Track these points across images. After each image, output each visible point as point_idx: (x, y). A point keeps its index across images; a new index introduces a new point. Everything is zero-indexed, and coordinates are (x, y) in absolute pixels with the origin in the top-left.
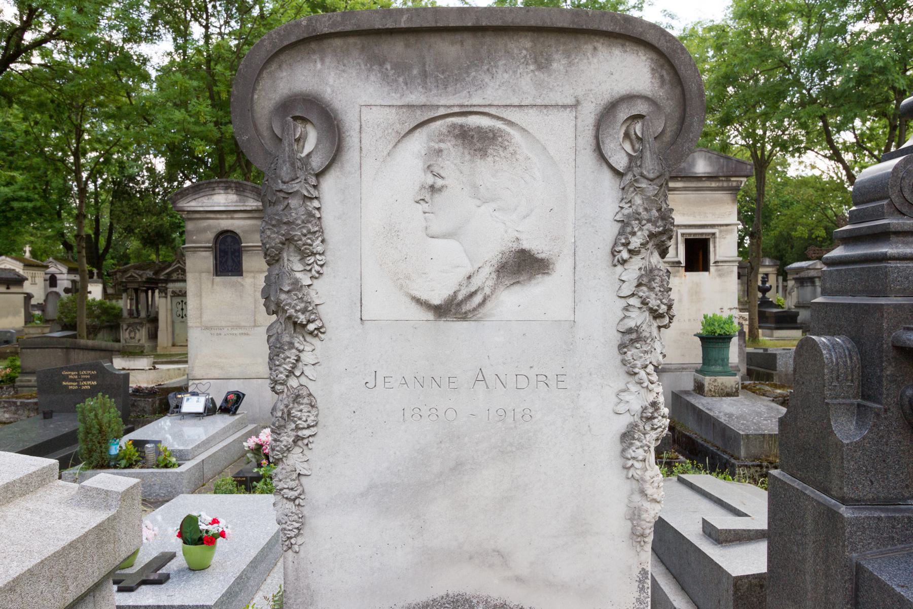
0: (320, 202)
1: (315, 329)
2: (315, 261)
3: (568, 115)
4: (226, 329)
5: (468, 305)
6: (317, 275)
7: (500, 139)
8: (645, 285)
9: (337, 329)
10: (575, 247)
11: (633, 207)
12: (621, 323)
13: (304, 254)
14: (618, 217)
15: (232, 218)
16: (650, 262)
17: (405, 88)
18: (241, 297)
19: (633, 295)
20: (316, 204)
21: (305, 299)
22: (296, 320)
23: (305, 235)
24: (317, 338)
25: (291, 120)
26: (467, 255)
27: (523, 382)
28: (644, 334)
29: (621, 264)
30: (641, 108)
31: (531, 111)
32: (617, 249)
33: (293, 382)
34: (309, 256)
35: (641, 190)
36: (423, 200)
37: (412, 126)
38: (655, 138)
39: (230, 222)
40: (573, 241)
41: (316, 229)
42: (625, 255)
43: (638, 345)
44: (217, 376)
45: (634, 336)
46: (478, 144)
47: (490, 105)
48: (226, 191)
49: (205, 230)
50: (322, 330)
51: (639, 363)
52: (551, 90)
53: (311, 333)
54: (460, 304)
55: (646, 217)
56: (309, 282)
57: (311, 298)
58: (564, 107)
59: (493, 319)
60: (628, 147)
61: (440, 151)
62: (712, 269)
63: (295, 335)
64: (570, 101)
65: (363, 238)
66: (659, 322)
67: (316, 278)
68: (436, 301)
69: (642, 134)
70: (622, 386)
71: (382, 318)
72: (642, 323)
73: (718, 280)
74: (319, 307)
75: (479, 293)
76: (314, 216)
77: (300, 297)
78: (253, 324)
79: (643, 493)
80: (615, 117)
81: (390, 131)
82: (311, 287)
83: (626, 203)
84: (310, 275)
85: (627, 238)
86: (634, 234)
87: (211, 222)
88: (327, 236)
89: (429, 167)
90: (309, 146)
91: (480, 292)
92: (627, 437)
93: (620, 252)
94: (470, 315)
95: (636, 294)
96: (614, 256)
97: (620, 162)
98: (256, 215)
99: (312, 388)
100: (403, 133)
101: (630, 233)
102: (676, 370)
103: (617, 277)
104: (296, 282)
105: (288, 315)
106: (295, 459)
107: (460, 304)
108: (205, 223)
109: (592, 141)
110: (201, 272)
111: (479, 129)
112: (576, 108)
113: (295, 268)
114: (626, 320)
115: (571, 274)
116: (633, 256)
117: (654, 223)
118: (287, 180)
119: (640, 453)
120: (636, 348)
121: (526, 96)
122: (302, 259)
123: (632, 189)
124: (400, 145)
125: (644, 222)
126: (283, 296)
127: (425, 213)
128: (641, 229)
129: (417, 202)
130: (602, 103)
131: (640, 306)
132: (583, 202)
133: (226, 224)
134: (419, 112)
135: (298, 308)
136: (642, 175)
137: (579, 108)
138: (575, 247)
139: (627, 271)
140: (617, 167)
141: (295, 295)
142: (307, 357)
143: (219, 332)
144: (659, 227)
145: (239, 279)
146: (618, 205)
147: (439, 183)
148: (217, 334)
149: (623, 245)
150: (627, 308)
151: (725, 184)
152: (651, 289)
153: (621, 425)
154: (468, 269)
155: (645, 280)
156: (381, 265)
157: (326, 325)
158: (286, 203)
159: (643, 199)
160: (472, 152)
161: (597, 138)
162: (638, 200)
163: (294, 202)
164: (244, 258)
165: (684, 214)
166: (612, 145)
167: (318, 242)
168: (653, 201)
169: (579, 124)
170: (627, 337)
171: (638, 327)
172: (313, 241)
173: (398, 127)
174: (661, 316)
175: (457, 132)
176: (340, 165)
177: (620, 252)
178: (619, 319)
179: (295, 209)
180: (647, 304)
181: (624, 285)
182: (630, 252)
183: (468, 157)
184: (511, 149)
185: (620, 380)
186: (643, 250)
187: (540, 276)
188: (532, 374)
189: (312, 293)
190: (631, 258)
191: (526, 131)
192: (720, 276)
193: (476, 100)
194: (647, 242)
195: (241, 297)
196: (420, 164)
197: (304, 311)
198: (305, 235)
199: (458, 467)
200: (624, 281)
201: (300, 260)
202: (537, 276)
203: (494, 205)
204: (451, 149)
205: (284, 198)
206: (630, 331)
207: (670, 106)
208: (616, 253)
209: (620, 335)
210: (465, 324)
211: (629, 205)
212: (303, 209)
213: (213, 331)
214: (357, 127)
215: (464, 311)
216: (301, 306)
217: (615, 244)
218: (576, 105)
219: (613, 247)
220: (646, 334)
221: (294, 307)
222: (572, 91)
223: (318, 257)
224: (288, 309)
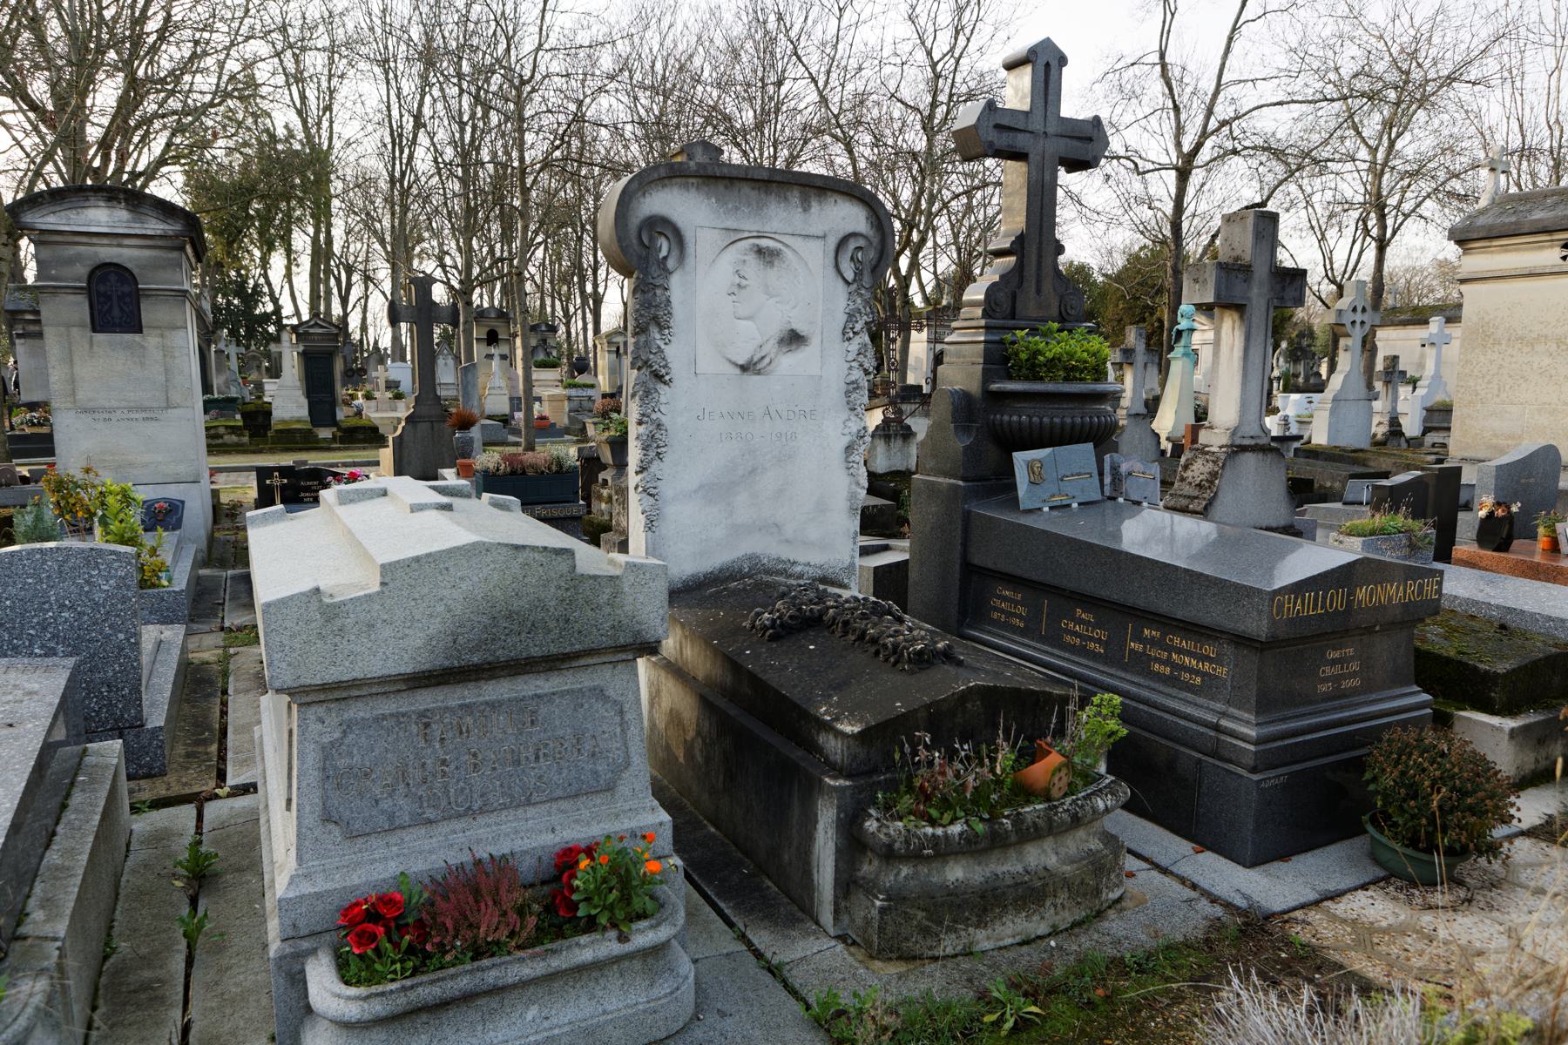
3: (819, 243)
4: (119, 412)
13: (661, 328)
15: (119, 245)
18: (142, 364)
30: (861, 242)
42: (851, 335)
48: (110, 204)
49: (70, 261)
53: (665, 383)
54: (755, 364)
64: (821, 234)
68: (741, 362)
70: (846, 417)
78: (164, 405)
79: (858, 484)
90: (664, 253)
92: (849, 449)
97: (850, 276)
98: (160, 243)
99: (664, 419)
104: (659, 347)
107: (755, 364)
108: (72, 251)
109: (833, 261)
110: (68, 326)
119: (857, 458)
133: (108, 253)
142: (663, 399)
143: (107, 416)
145: (137, 337)
147: (744, 282)
148: (105, 420)
150: (851, 368)
153: (845, 441)
154: (759, 341)
161: (836, 258)
162: (859, 301)
163: (659, 292)
164: (143, 306)
170: (851, 387)
182: (855, 333)
185: (845, 414)
188: (796, 410)
193: (767, 228)
195: (142, 364)
199: (753, 471)
203: (775, 299)
206: (853, 382)
207: (875, 241)
213: (96, 416)
218: (824, 237)
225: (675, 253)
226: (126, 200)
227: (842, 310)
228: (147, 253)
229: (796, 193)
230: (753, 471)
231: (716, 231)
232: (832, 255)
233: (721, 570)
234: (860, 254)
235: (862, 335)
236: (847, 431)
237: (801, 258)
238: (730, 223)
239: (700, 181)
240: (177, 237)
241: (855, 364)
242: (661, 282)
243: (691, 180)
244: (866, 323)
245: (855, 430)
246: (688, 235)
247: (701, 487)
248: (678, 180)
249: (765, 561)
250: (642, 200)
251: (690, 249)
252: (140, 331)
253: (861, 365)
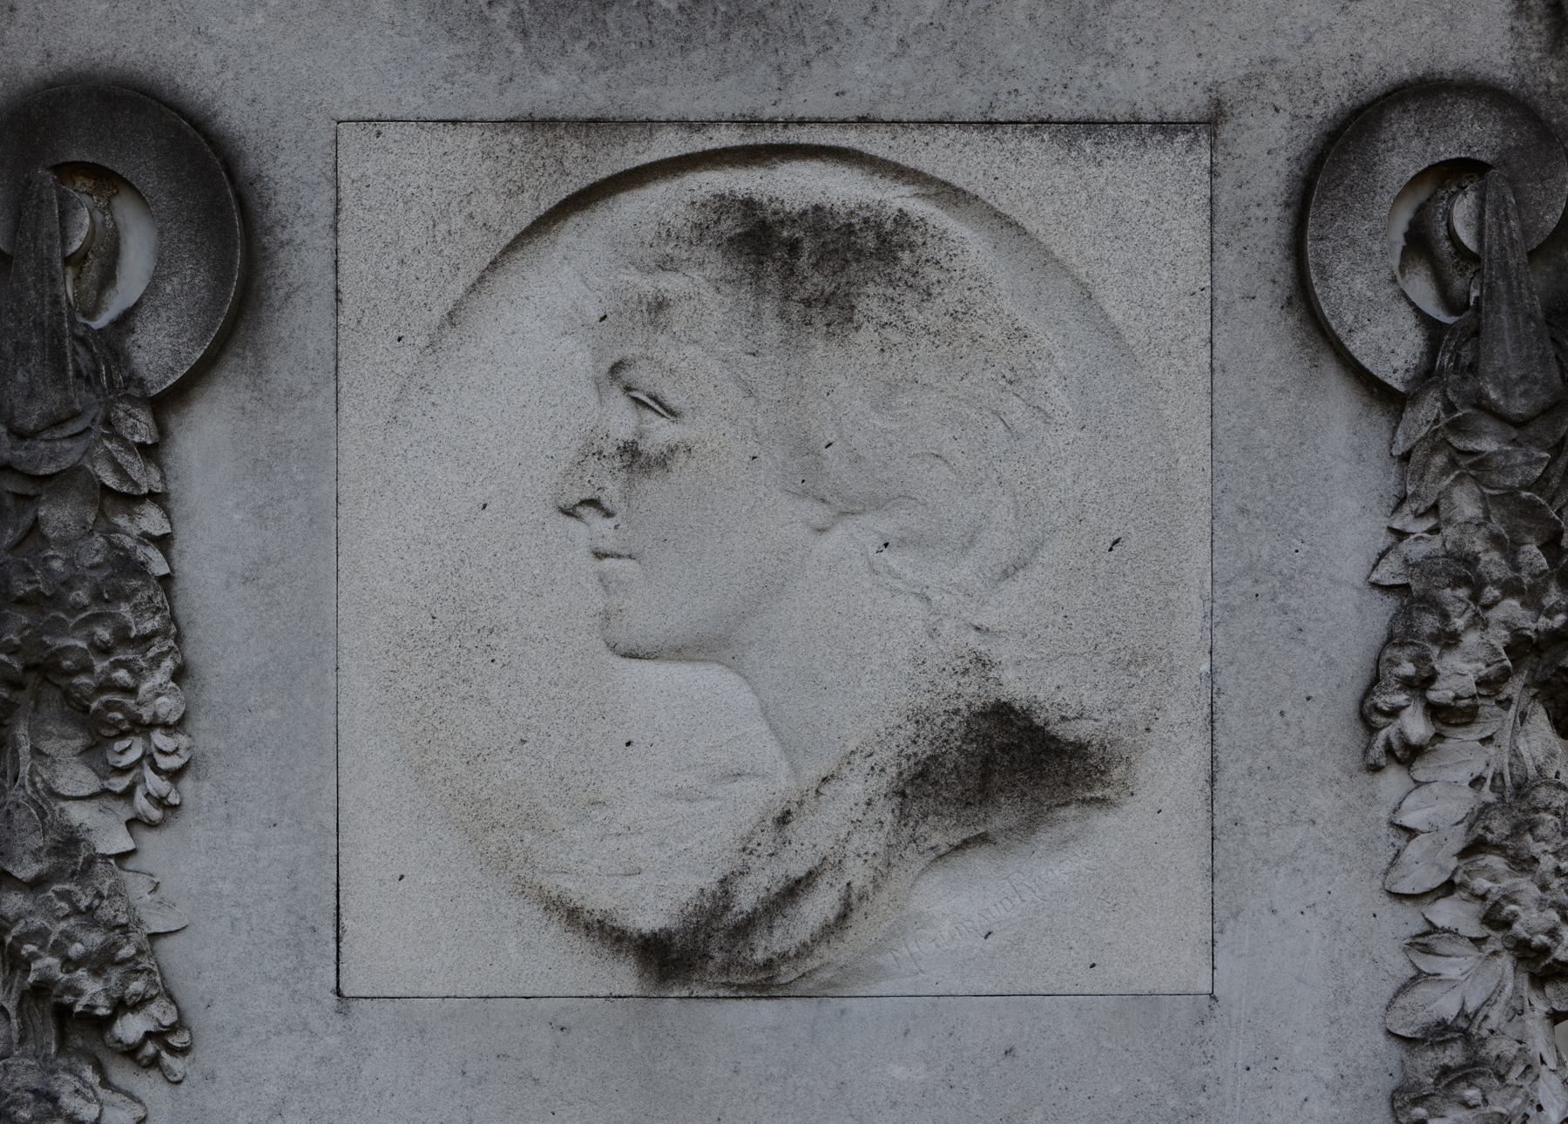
0: (168, 515)
1: (148, 1035)
2: (148, 758)
5: (778, 933)
6: (156, 814)
7: (906, 257)
8: (1499, 848)
9: (238, 1033)
10: (1215, 692)
11: (1449, 532)
12: (1401, 1001)
14: (1389, 572)
16: (1516, 754)
17: (518, 48)
19: (1449, 888)
20: (152, 520)
21: (106, 912)
22: (68, 999)
23: (104, 650)
24: (154, 1074)
25: (51, 178)
26: (774, 729)
28: (1494, 1047)
29: (1399, 762)
31: (1029, 144)
32: (1385, 701)
34: (123, 735)
35: (1478, 467)
36: (593, 503)
37: (545, 206)
38: (1531, 254)
40: (1205, 667)
41: (150, 624)
42: (1416, 726)
43: (1472, 1094)
45: (1453, 1055)
46: (817, 278)
47: (864, 121)
50: (176, 1041)
52: (1112, 60)
53: (131, 1053)
54: (745, 928)
55: (1496, 575)
56: (123, 842)
57: (130, 909)
58: (1166, 127)
59: (885, 987)
60: (1422, 289)
61: (660, 305)
63: (62, 1061)
64: (1185, 102)
65: (345, 660)
67: (152, 825)
68: (649, 918)
69: (1480, 236)
71: (426, 989)
72: (1488, 1002)
74: (164, 945)
75: (822, 883)
76: (140, 569)
77: (84, 903)
80: (1368, 169)
81: (458, 222)
82: (131, 864)
83: (1419, 516)
84: (127, 814)
85: (1421, 659)
86: (1449, 640)
88: (196, 652)
89: (616, 368)
91: (827, 877)
93: (1394, 712)
94: (786, 974)
95: (1463, 885)
96: (1372, 730)
100: (511, 232)
101: (1435, 639)
103: (1384, 814)
104: (69, 842)
105: (31, 978)
107: (745, 928)
109: (1277, 261)
112: (1213, 135)
113: (65, 785)
114: (1422, 992)
115: (1199, 802)
116: (1449, 731)
117: (1531, 597)
118: (31, 423)
120: (1465, 1104)
121: (1014, 84)
122: (94, 751)
123: (1439, 460)
124: (498, 280)
125: (1491, 593)
126: (15, 902)
127: (600, 555)
128: (1480, 623)
129: (569, 512)
130: (1318, 112)
131: (1476, 930)
132: (1243, 511)
134: (574, 148)
135: (76, 949)
136: (1482, 405)
137: (1226, 132)
138: (1215, 692)
139: (1424, 791)
140: (1381, 371)
141: (65, 896)
144: (1550, 613)
146: (1384, 522)
147: (661, 432)
149: (1407, 684)
150: (1425, 941)
152: (1523, 863)
154: (782, 785)
155: (1499, 827)
156: (420, 771)
157: (195, 1018)
158: (27, 520)
159: (1483, 498)
160: (795, 309)
161: (1297, 249)
162: (1465, 503)
163: (59, 516)
166: (1359, 284)
167: (160, 677)
168: (1530, 509)
169: (1223, 199)
170: (1429, 1060)
171: (1470, 1018)
172: (137, 674)
173: (491, 207)
175: (730, 226)
176: (250, 361)
177: (1394, 712)
178: (1389, 989)
179: (65, 543)
180: (1507, 924)
181: (1414, 849)
182: (1436, 712)
183: (773, 330)
184: (949, 298)
186: (1488, 708)
187: (1072, 811)
189: (137, 888)
190: (1439, 737)
191: (1011, 224)
193: (809, 98)
194: (1505, 675)
196: (581, 360)
197: (100, 963)
198: (104, 650)
200: (1411, 833)
201: (87, 750)
202: (1062, 813)
203: (886, 526)
204: (708, 295)
205: (18, 497)
206: (1439, 1034)
208: (1380, 720)
209: (1397, 1051)
210: (766, 1011)
211: (1430, 523)
212: (99, 541)
214: (321, 204)
215: (760, 956)
216: (91, 940)
217: (1376, 680)
219: (1368, 692)
220: (1502, 1046)
221: (58, 949)
222: (1194, 66)
223: (159, 739)
224: (34, 956)
225: (190, 279)
227: (1353, 568)
231: (472, 139)
234: (1463, 212)
235: (1493, 720)
237: (1049, 261)
242: (70, 454)
244: (1520, 647)
253: (1496, 920)
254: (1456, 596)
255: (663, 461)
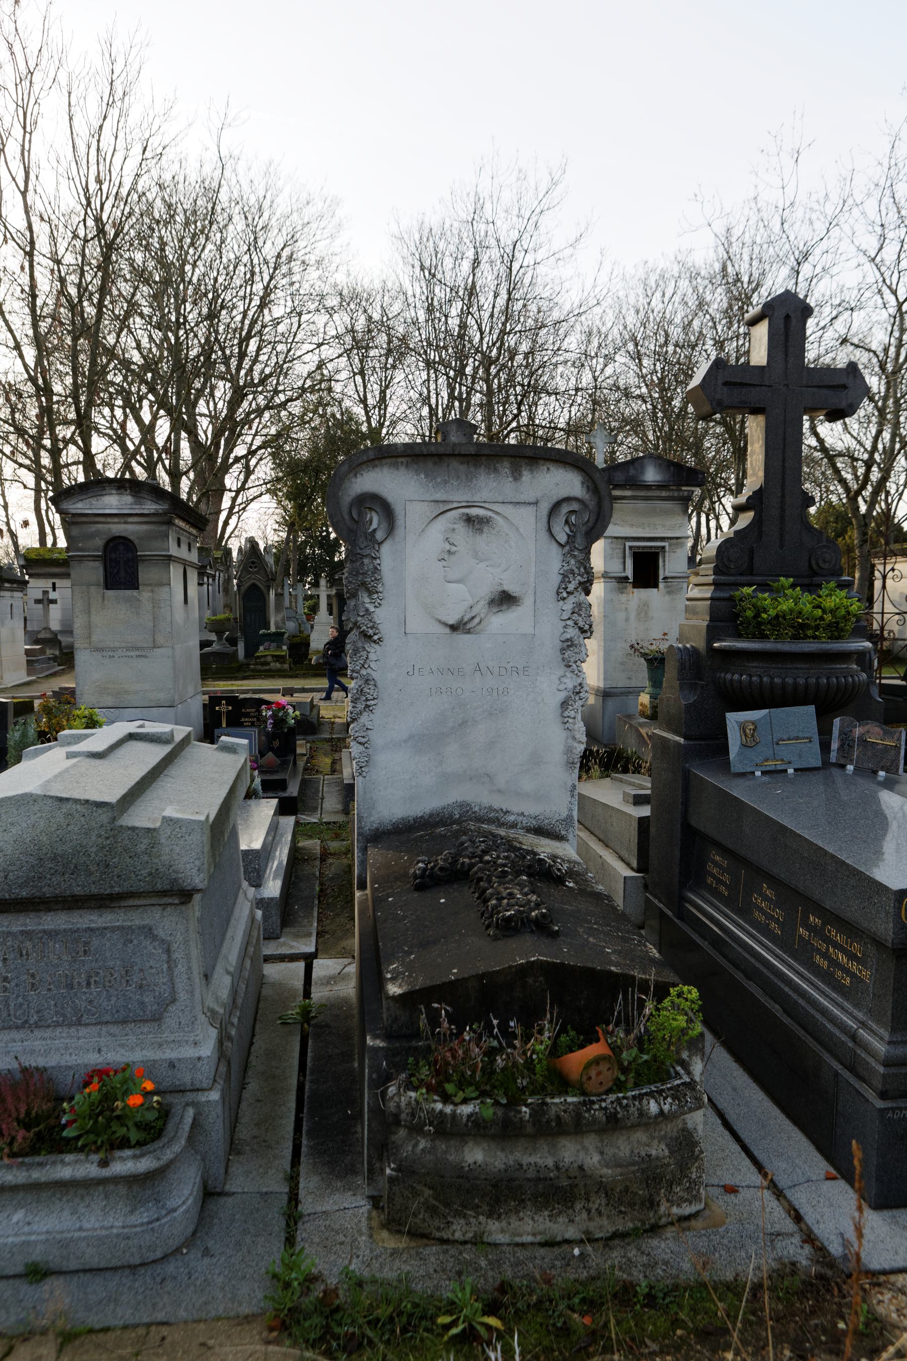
3: (531, 510)
13: (370, 593)
15: (126, 523)
18: (138, 614)
27: (503, 672)
30: (575, 506)
33: (364, 672)
35: (575, 556)
39: (123, 527)
42: (565, 595)
44: (110, 705)
49: (92, 536)
51: (572, 660)
53: (375, 642)
54: (465, 624)
58: (529, 504)
60: (567, 529)
62: (661, 585)
64: (532, 500)
66: (584, 635)
68: (451, 622)
70: (562, 673)
73: (667, 598)
79: (574, 738)
87: (112, 526)
90: (374, 525)
92: (565, 704)
97: (563, 538)
98: (153, 519)
99: (374, 675)
102: (622, 694)
104: (367, 610)
106: (364, 719)
107: (465, 624)
108: (94, 528)
109: (546, 524)
110: (89, 585)
111: (477, 516)
117: (582, 576)
119: (572, 714)
126: (359, 619)
133: (118, 529)
142: (372, 656)
143: (111, 654)
145: (134, 593)
147: (454, 549)
150: (565, 627)
151: (676, 494)
152: (580, 615)
153: (562, 696)
154: (471, 602)
162: (573, 562)
163: (366, 561)
165: (632, 525)
174: (586, 631)
185: (561, 671)
188: (508, 666)
192: (669, 593)
195: (138, 614)
197: (372, 628)
199: (464, 723)
206: (567, 640)
207: (592, 504)
210: (469, 636)
213: (105, 653)
218: (536, 503)
225: (384, 525)
226: (131, 488)
228: (145, 527)
229: (506, 464)
230: (464, 723)
232: (544, 519)
233: (431, 815)
235: (576, 594)
236: (562, 687)
238: (439, 496)
239: (409, 459)
240: (165, 514)
241: (570, 623)
242: (368, 552)
243: (400, 460)
245: (570, 686)
246: (398, 509)
247: (411, 737)
248: (388, 460)
249: (477, 809)
250: (353, 480)
251: (400, 521)
252: (137, 588)
253: (576, 624)
254: (571, 576)
255: (454, 553)
